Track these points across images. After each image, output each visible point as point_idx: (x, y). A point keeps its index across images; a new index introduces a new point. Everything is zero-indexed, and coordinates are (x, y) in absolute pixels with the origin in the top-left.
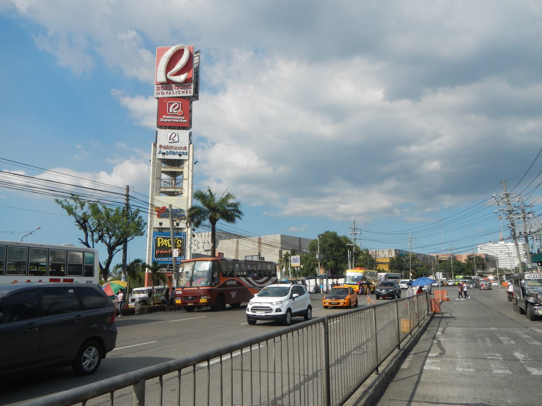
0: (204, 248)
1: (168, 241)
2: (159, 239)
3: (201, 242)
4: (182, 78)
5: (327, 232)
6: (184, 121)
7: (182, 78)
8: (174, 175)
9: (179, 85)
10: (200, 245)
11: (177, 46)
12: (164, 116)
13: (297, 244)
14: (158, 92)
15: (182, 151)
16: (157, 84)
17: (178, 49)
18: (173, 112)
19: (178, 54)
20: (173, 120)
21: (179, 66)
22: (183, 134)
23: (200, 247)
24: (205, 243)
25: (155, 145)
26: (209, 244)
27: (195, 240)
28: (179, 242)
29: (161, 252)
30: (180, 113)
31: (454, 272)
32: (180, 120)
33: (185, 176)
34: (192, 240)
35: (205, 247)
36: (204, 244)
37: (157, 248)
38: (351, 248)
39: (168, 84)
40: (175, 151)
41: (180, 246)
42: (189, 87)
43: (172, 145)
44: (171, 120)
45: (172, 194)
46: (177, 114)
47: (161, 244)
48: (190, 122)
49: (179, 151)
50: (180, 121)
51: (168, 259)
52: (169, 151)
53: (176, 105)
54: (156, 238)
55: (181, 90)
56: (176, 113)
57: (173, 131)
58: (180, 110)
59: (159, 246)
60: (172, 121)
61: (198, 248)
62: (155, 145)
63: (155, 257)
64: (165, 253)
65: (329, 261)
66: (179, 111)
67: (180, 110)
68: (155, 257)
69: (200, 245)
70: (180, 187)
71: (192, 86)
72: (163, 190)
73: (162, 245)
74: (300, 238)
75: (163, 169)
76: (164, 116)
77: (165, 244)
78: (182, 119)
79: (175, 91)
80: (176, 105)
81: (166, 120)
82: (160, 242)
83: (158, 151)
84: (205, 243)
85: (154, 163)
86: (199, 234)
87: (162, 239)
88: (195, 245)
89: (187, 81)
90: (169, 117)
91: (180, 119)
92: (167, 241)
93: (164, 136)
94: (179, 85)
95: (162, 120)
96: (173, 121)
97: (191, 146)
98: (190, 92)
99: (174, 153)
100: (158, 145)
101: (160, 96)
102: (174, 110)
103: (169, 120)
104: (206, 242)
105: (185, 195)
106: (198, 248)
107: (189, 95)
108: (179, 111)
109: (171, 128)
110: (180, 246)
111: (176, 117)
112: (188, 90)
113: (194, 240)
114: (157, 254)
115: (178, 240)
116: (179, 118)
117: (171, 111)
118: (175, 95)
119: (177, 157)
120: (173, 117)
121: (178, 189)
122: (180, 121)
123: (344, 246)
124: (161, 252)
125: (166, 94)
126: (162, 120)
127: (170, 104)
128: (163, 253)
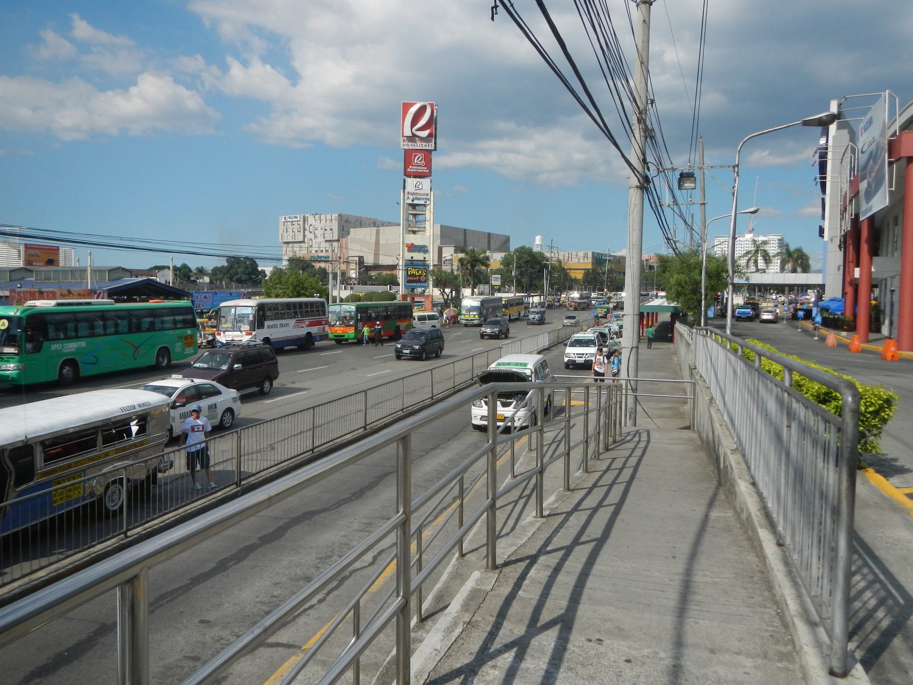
0: (324, 237)
3: (319, 229)
4: (424, 134)
5: (523, 248)
7: (424, 134)
8: (415, 215)
9: (422, 139)
10: (319, 233)
13: (461, 238)
14: (404, 143)
15: (425, 197)
19: (422, 110)
21: (423, 122)
22: (426, 183)
23: (319, 236)
24: (326, 230)
25: (404, 192)
26: (331, 232)
27: (311, 225)
29: (411, 279)
30: (423, 164)
31: (656, 286)
33: (428, 219)
34: (306, 225)
35: (326, 236)
36: (325, 232)
38: (546, 266)
39: (413, 138)
40: (420, 197)
42: (430, 141)
43: (417, 191)
45: (414, 232)
48: (430, 172)
49: (423, 197)
52: (415, 197)
53: (419, 157)
55: (424, 144)
57: (418, 180)
58: (423, 162)
61: (316, 237)
62: (404, 192)
65: (523, 278)
67: (423, 162)
69: (319, 233)
70: (424, 226)
71: (433, 141)
72: (410, 229)
74: (465, 230)
75: (410, 212)
76: (410, 167)
79: (418, 144)
80: (419, 157)
81: (412, 170)
83: (406, 197)
84: (326, 230)
85: (403, 207)
86: (317, 216)
88: (311, 232)
89: (430, 135)
90: (415, 167)
93: (411, 182)
94: (422, 139)
95: (409, 170)
97: (432, 192)
98: (431, 146)
99: (419, 199)
100: (406, 191)
101: (406, 147)
103: (414, 170)
104: (328, 230)
105: (428, 234)
106: (316, 237)
107: (430, 148)
109: (415, 177)
111: (420, 168)
112: (430, 144)
113: (309, 224)
116: (422, 168)
117: (415, 162)
118: (418, 148)
119: (422, 202)
121: (422, 228)
123: (539, 263)
125: (411, 146)
127: (416, 155)
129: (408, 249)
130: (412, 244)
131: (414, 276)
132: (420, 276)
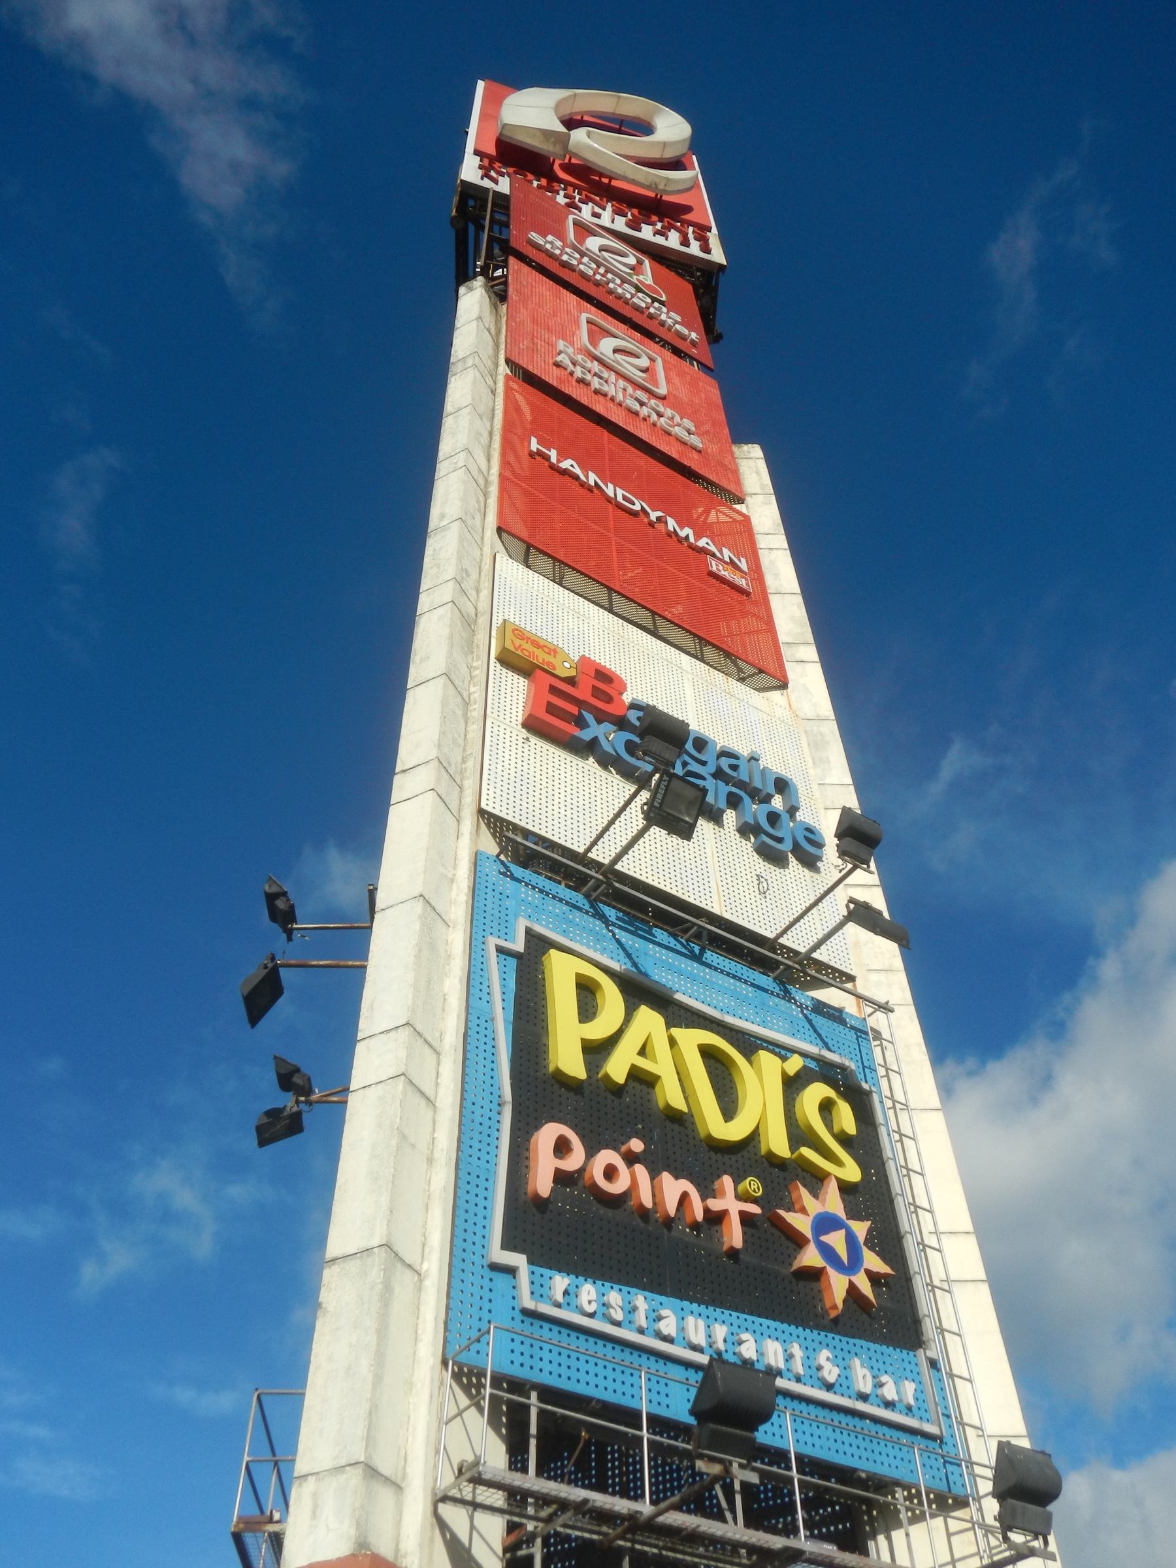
1: (691, 1039)
12: (550, 238)
16: (477, 152)
30: (648, 287)
41: (852, 1172)
47: (596, 1051)
51: (720, 1332)
54: (519, 946)
63: (508, 1244)
68: (508, 1244)
73: (617, 1068)
82: (587, 1009)
87: (612, 999)
110: (852, 1172)
114: (543, 1183)
124: (610, 1173)
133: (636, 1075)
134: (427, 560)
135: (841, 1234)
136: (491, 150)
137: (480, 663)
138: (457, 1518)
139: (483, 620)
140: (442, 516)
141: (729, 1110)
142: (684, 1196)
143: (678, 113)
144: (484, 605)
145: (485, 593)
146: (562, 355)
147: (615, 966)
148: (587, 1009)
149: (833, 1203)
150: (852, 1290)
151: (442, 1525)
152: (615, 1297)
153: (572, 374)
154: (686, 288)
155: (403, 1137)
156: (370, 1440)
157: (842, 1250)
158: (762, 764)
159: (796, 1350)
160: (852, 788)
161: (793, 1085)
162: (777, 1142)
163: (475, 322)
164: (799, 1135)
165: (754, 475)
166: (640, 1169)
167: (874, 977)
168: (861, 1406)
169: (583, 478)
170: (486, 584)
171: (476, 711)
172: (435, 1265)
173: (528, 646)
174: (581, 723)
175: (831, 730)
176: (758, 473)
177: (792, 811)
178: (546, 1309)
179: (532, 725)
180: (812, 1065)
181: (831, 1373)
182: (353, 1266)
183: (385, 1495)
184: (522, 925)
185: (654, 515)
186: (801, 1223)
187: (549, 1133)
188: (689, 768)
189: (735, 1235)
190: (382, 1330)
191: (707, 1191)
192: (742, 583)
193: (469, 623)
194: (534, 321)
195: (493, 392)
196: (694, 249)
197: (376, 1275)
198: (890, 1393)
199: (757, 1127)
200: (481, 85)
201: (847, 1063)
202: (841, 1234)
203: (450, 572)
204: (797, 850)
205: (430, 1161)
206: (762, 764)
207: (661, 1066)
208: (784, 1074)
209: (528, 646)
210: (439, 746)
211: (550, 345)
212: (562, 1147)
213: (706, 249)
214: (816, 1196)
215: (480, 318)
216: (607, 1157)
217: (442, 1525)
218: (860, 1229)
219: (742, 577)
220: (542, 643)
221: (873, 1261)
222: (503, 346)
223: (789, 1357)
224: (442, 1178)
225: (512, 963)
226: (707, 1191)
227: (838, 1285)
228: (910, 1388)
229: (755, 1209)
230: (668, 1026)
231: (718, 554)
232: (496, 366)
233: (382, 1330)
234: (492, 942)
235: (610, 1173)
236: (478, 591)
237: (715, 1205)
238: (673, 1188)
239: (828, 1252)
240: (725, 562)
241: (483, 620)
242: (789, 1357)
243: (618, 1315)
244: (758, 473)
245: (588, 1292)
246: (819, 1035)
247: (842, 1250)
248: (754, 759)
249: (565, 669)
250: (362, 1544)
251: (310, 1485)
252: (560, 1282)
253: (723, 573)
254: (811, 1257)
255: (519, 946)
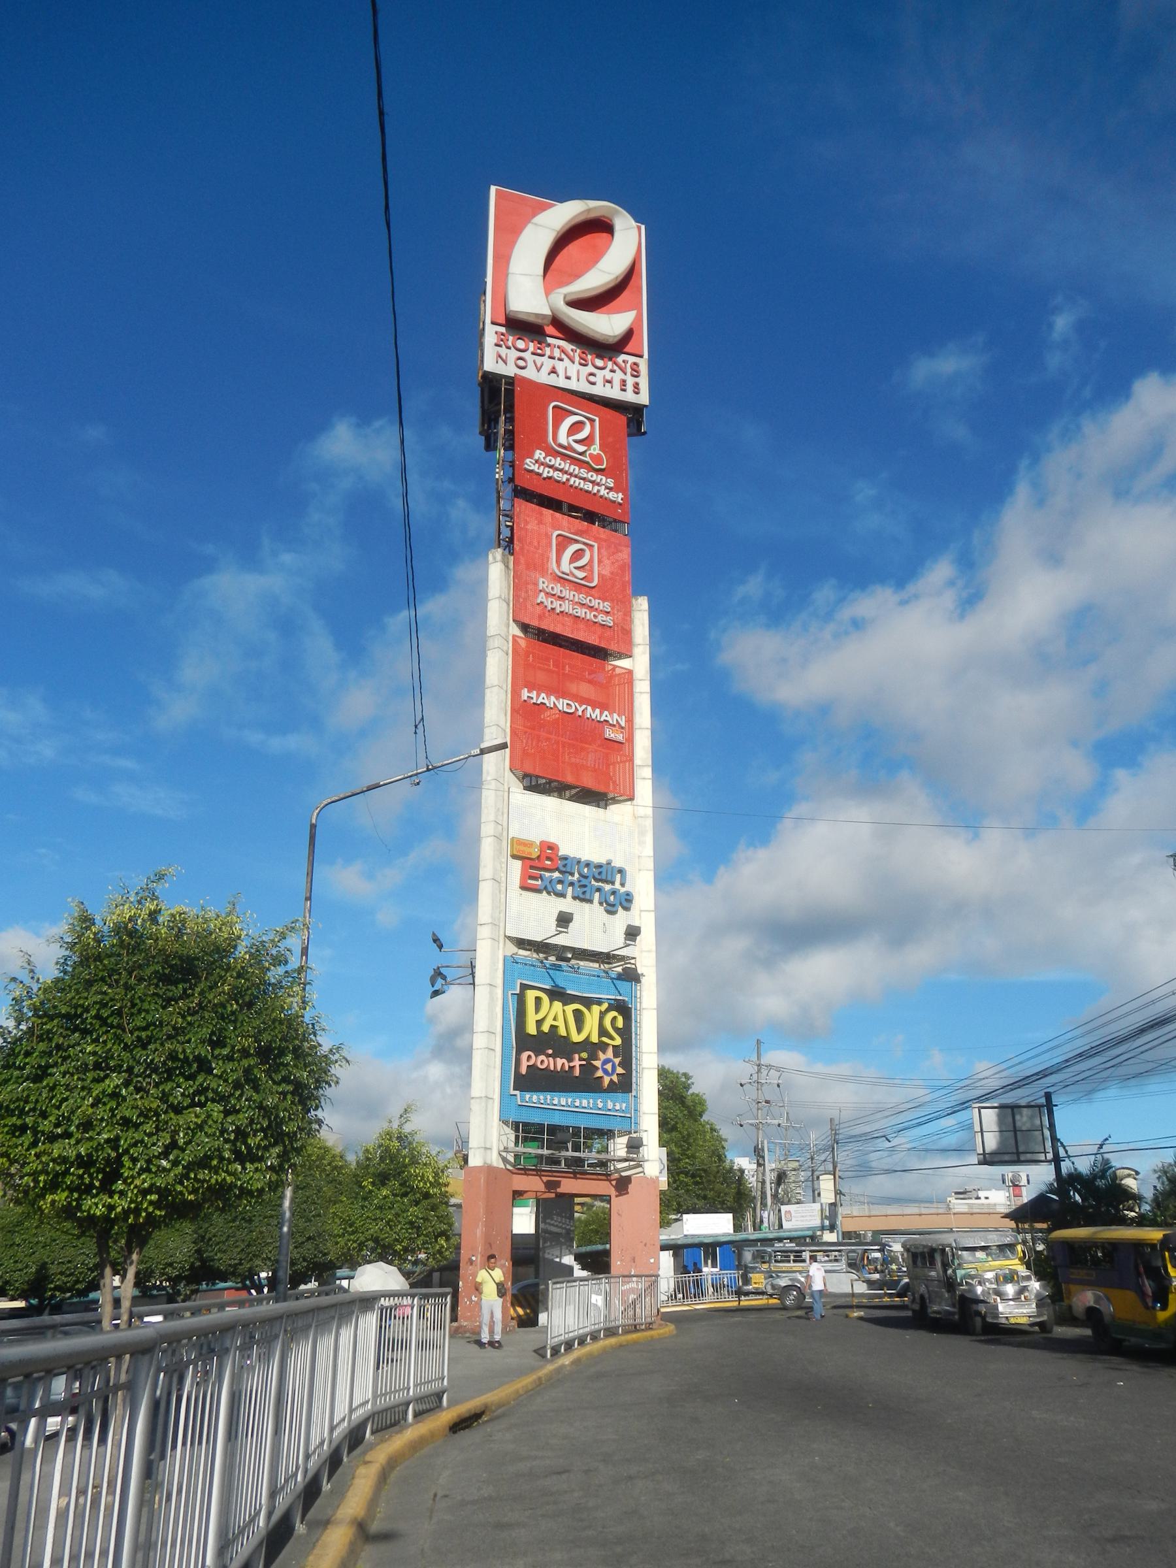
1: (570, 1008)
2: (531, 995)
6: (612, 496)
11: (593, 204)
12: (539, 454)
16: (493, 323)
17: (593, 215)
18: (569, 448)
20: (573, 479)
28: (614, 1018)
29: (544, 1062)
32: (596, 488)
37: (524, 1042)
41: (618, 1041)
44: (565, 477)
46: (587, 459)
47: (539, 1023)
50: (598, 491)
51: (570, 1100)
54: (518, 992)
56: (581, 454)
59: (532, 1029)
60: (568, 480)
63: (514, 1089)
64: (559, 1070)
66: (592, 451)
67: (595, 449)
68: (514, 1089)
73: (546, 1028)
76: (539, 454)
77: (555, 1023)
78: (607, 488)
81: (546, 472)
82: (537, 1009)
87: (545, 999)
91: (598, 484)
92: (564, 1011)
96: (571, 482)
102: (576, 441)
103: (557, 475)
108: (592, 451)
110: (618, 1041)
111: (583, 473)
114: (524, 1070)
115: (607, 1010)
117: (563, 438)
118: (573, 385)
120: (572, 467)
122: (598, 491)
124: (542, 1062)
126: (532, 467)
127: (560, 414)
128: (552, 1068)
129: (526, 876)
130: (552, 847)
131: (550, 1042)
132: (591, 1048)
133: (552, 1026)
134: (483, 801)
135: (611, 1064)
136: (502, 320)
137: (504, 860)
138: (504, 1154)
139: (505, 833)
140: (488, 773)
141: (579, 1030)
142: (563, 1064)
143: (629, 213)
144: (505, 824)
145: (506, 815)
146: (542, 594)
147: (547, 987)
148: (537, 1009)
149: (610, 1053)
150: (611, 1079)
151: (500, 1155)
152: (542, 1097)
153: (546, 607)
154: (621, 420)
155: (488, 1066)
156: (485, 1142)
157: (610, 1070)
158: (613, 865)
159: (591, 1101)
160: (652, 859)
161: (602, 1015)
162: (595, 1039)
163: (497, 600)
164: (603, 1032)
165: (641, 627)
166: (551, 1059)
167: (645, 954)
168: (608, 1113)
169: (548, 705)
170: (506, 811)
171: (503, 889)
172: (497, 1097)
173: (522, 848)
174: (541, 877)
175: (649, 823)
176: (643, 625)
177: (623, 885)
178: (524, 1104)
179: (524, 888)
180: (612, 1002)
181: (600, 1105)
182: (478, 1100)
183: (489, 1151)
184: (519, 982)
185: (580, 710)
186: (597, 1063)
187: (525, 1055)
188: (582, 883)
189: (577, 1072)
190: (486, 1115)
191: (570, 1060)
192: (620, 737)
193: (498, 838)
194: (528, 568)
195: (507, 654)
196: (629, 397)
197: (483, 1104)
198: (618, 1107)
199: (589, 1035)
200: (493, 189)
201: (625, 998)
202: (611, 1064)
203: (492, 818)
204: (621, 904)
205: (495, 1067)
206: (613, 865)
207: (560, 1023)
208: (601, 1012)
209: (522, 848)
210: (492, 917)
211: (536, 584)
212: (529, 1057)
213: (636, 388)
214: (604, 1053)
215: (500, 597)
216: (542, 1057)
217: (500, 1155)
218: (617, 1061)
219: (622, 732)
220: (527, 842)
221: (620, 1070)
222: (511, 611)
223: (589, 1103)
224: (498, 1073)
225: (516, 996)
226: (570, 1060)
227: (607, 1080)
228: (624, 1105)
229: (584, 1063)
230: (563, 1006)
231: (611, 722)
232: (508, 626)
233: (486, 1115)
234: (510, 992)
235: (542, 1062)
236: (503, 814)
237: (572, 1064)
238: (560, 1062)
239: (605, 1071)
240: (614, 726)
241: (505, 833)
242: (589, 1103)
243: (542, 1102)
244: (643, 625)
245: (535, 1098)
246: (617, 989)
247: (610, 1070)
248: (609, 863)
249: (535, 853)
250: (485, 1163)
251: (473, 1150)
252: (528, 1096)
253: (612, 735)
254: (600, 1073)
255: (518, 992)
